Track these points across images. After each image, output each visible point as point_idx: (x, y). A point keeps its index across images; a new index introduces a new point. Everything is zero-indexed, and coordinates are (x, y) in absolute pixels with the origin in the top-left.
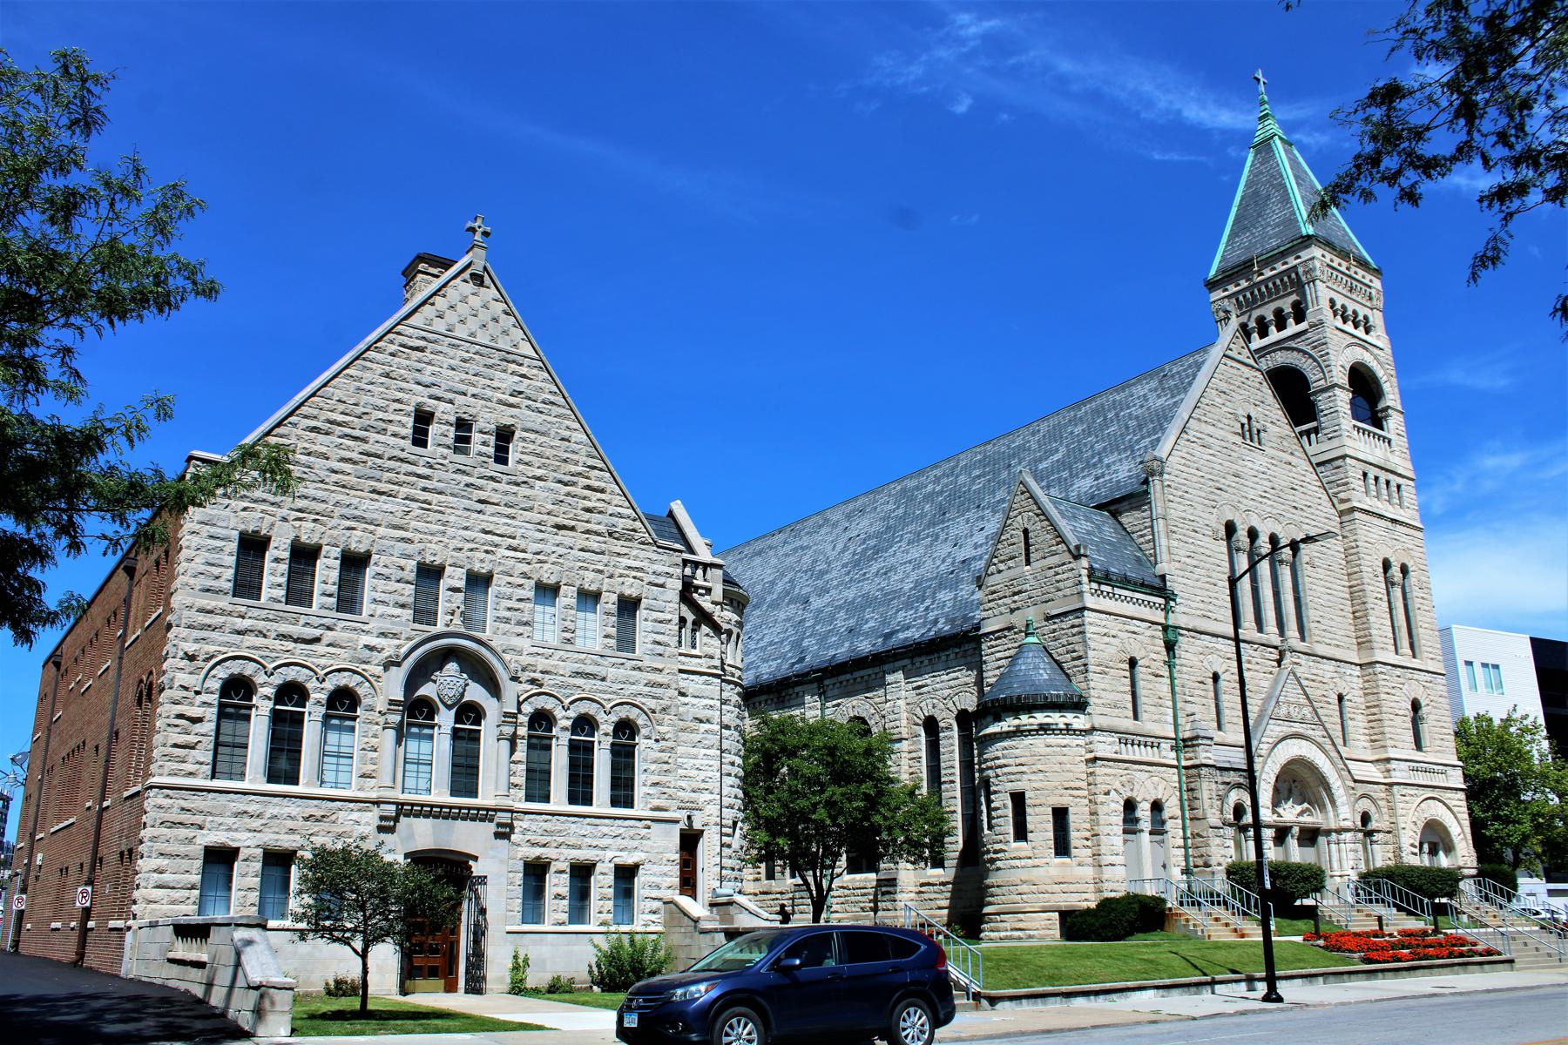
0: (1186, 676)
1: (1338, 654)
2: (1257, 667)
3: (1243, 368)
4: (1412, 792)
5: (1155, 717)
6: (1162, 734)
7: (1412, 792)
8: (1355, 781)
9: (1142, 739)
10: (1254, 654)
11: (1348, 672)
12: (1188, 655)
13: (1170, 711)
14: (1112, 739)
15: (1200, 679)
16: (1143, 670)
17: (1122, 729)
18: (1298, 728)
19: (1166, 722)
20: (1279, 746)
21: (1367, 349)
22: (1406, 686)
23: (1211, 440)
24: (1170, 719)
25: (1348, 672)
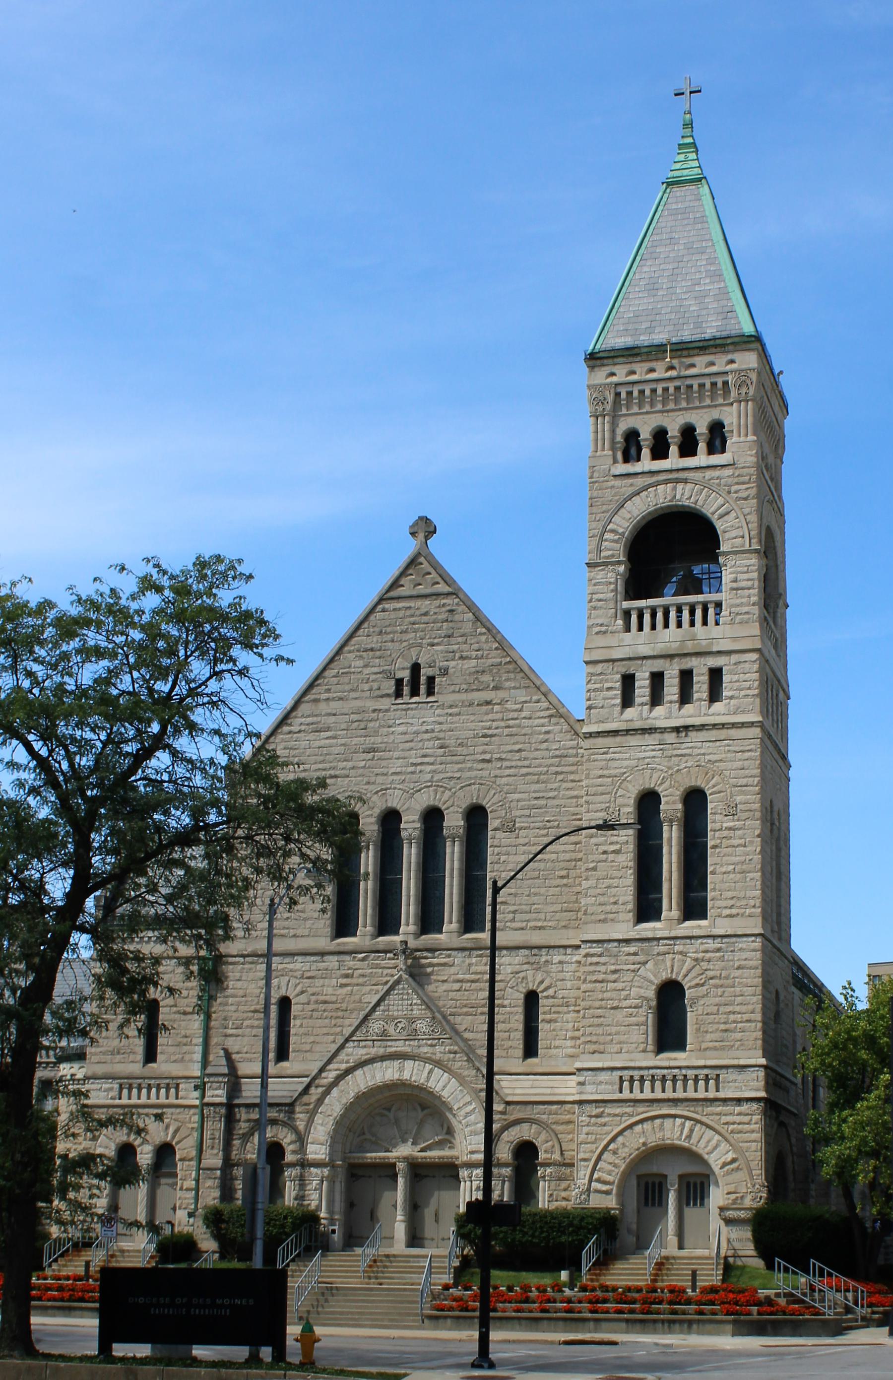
0: (233, 1008)
1: (536, 938)
2: (361, 980)
3: (419, 603)
4: (618, 1111)
5: (173, 1058)
6: (181, 1074)
7: (618, 1111)
8: (508, 1103)
9: (152, 1082)
10: (359, 964)
11: (556, 959)
12: (239, 984)
13: (199, 1049)
14: (108, 1086)
15: (252, 1008)
16: (167, 1010)
17: (122, 1075)
18: (399, 1047)
19: (191, 1061)
20: (359, 1073)
21: (685, 481)
22: (650, 965)
23: (332, 719)
24: (198, 1056)
25: (556, 959)
